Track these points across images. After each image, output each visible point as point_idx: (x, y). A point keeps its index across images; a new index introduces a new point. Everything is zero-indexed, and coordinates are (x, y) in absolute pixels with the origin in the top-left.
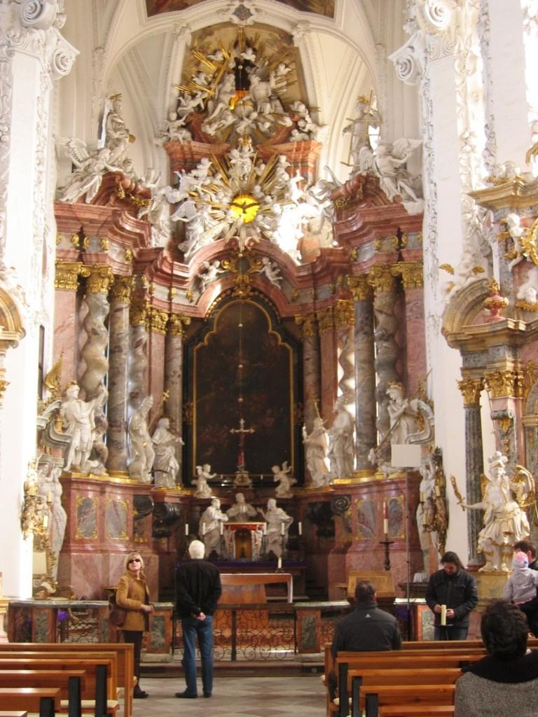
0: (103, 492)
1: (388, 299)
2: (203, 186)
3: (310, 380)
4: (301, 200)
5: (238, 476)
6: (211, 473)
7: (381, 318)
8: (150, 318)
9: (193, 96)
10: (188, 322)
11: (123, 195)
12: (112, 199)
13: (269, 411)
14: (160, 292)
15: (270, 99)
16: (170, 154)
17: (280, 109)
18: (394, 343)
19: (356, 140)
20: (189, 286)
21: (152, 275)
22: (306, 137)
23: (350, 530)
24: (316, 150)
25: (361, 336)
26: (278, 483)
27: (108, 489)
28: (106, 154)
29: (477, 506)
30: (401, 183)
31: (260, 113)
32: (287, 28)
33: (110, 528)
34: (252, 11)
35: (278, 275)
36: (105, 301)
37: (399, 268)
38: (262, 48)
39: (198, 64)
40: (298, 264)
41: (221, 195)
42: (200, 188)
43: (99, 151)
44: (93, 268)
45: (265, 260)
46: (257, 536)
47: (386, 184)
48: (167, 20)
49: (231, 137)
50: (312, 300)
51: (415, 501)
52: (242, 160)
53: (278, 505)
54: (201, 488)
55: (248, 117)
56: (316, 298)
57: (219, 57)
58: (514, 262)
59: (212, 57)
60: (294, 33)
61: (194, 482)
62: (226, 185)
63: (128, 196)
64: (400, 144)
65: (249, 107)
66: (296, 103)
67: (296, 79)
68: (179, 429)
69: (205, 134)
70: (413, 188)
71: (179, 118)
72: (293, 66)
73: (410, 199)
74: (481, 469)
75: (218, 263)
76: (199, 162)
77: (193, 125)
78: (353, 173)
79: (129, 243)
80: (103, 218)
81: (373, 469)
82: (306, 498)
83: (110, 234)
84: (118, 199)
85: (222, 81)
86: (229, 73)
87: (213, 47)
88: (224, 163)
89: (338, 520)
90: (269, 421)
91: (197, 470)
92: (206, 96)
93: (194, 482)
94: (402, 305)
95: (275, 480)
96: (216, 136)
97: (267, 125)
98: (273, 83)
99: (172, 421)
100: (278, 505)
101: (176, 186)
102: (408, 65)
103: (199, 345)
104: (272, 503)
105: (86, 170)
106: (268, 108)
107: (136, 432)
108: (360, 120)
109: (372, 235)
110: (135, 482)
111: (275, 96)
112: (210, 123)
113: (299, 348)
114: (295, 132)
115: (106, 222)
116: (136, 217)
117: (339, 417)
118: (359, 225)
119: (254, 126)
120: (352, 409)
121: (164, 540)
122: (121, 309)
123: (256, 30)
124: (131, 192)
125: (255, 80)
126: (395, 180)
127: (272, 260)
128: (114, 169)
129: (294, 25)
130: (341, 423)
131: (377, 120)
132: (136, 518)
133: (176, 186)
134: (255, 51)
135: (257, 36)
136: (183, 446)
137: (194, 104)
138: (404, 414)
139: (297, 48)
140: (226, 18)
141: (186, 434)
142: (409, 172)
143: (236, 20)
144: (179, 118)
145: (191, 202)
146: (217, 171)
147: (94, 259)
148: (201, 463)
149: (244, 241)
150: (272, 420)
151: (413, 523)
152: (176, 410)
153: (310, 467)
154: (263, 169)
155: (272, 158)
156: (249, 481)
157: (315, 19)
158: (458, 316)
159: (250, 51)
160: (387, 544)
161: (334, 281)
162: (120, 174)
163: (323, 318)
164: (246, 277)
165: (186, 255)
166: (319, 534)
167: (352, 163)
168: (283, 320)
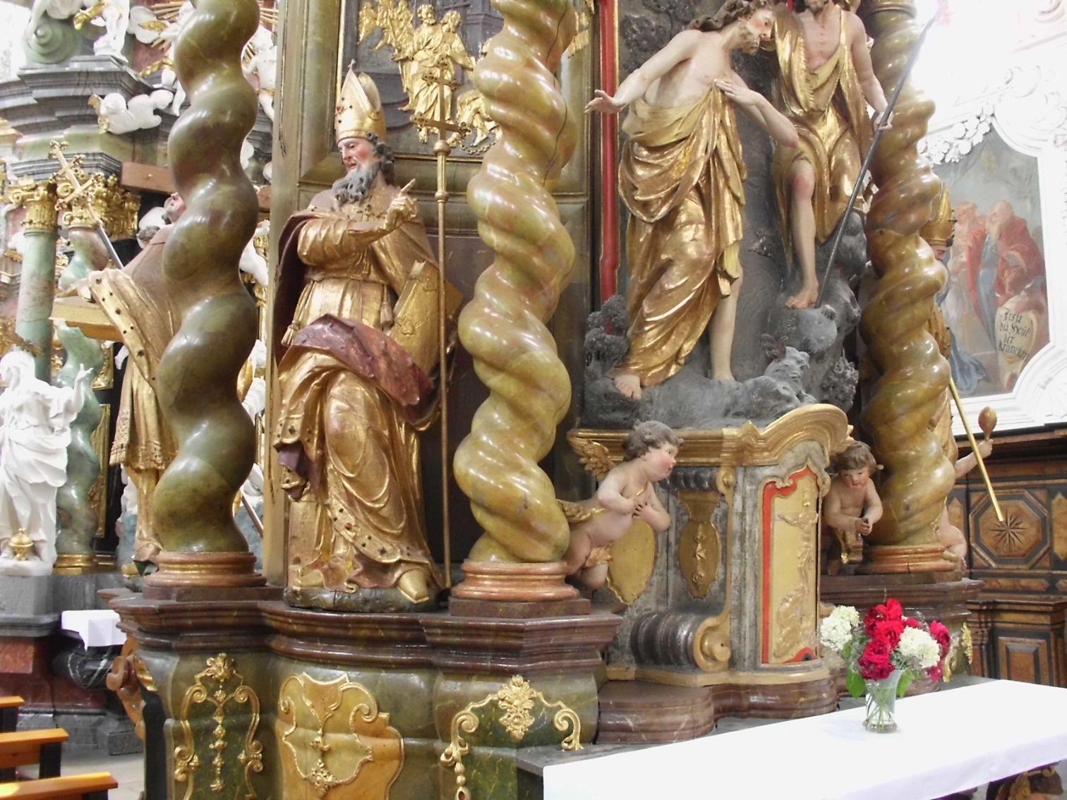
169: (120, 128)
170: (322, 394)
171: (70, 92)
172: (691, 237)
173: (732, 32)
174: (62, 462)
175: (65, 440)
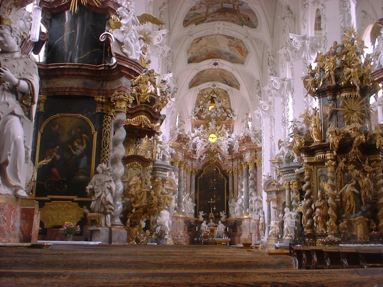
0: (177, 219)
1: (253, 169)
2: (201, 132)
3: (230, 188)
4: (229, 137)
5: (210, 215)
6: (203, 214)
7: (251, 174)
8: (187, 170)
9: (199, 107)
10: (197, 171)
11: (183, 140)
12: (180, 140)
13: (219, 196)
14: (189, 163)
15: (220, 108)
16: (192, 123)
17: (223, 111)
18: (254, 181)
19: (245, 126)
20: (197, 161)
21: (187, 158)
22: (231, 119)
23: (241, 230)
24: (233, 123)
25: (245, 178)
26: (222, 217)
27: (178, 218)
28: (178, 129)
29: (269, 226)
30: (256, 139)
31: (218, 112)
32: (226, 90)
33: (179, 229)
34: (216, 85)
35: (222, 158)
36: (178, 168)
37: (256, 161)
38: (219, 94)
39: (201, 98)
40: (228, 156)
41: (206, 135)
42: (200, 133)
43: (177, 128)
44: (175, 159)
45: (218, 154)
46: (216, 231)
47: (252, 138)
48: (193, 89)
49: (209, 119)
50: (232, 166)
51: (258, 224)
52: (212, 125)
53: (222, 223)
54: (200, 218)
55: (214, 113)
56: (233, 165)
57: (207, 96)
58: (278, 175)
59: (204, 96)
60: (228, 92)
61: (198, 216)
62: (208, 132)
63: (184, 140)
64: (257, 128)
65: (215, 110)
66: (228, 110)
67: (228, 102)
68: (194, 201)
69: (202, 117)
70: (260, 140)
71: (195, 113)
72: (227, 99)
73: (259, 143)
74: (270, 218)
75: (205, 154)
76: (200, 125)
77: (198, 116)
78: (244, 134)
79: (183, 152)
80: (178, 146)
81: (248, 214)
82: (229, 221)
83: (179, 150)
84: (181, 141)
85: (207, 102)
86: (209, 100)
87: (206, 93)
88: (207, 126)
89: (238, 227)
90: (219, 199)
91: (199, 213)
92: (202, 107)
93: (198, 216)
94: (256, 170)
95: (221, 216)
96: (205, 118)
97: (220, 115)
98: (221, 103)
99: (192, 199)
100: (222, 223)
101: (194, 132)
102: (258, 115)
103: (200, 177)
104: (220, 222)
105: (173, 133)
106: (220, 110)
107: (185, 203)
108: (246, 119)
109: (249, 151)
110: (185, 216)
111: (222, 107)
112: (204, 115)
113: (228, 179)
114: (227, 117)
115: (178, 147)
116: (185, 145)
117: (239, 200)
118: (245, 149)
119: (216, 115)
120: (243, 197)
121: (190, 232)
122: (181, 170)
123: (217, 90)
124: (184, 139)
125: (216, 102)
126: (255, 138)
127: (220, 154)
128: (181, 133)
129: (228, 90)
130: (240, 201)
131: (251, 120)
132: (184, 226)
133: (194, 132)
134: (217, 95)
135: (218, 91)
136: (195, 206)
137: (199, 109)
138: (257, 200)
139: (229, 95)
140: (209, 87)
141: (196, 202)
142: (258, 136)
143: (212, 87)
144: (195, 113)
145: (198, 137)
146: (205, 128)
147: (175, 157)
148: (201, 211)
149: (212, 148)
150: (220, 199)
151: (258, 228)
152: (194, 196)
153: (230, 212)
154: (218, 128)
155: (221, 125)
156: (213, 216)
157: (234, 89)
158: (266, 186)
159: (215, 95)
160: (251, 234)
161: (238, 161)
162: (182, 134)
163: (234, 171)
164: (213, 158)
165: (197, 152)
166: (233, 231)
167: (244, 131)
168: (223, 171)
169: (298, 173)
170: (317, 218)
171: (291, 169)
172: (348, 203)
173: (351, 184)
174: (294, 224)
175: (294, 221)
